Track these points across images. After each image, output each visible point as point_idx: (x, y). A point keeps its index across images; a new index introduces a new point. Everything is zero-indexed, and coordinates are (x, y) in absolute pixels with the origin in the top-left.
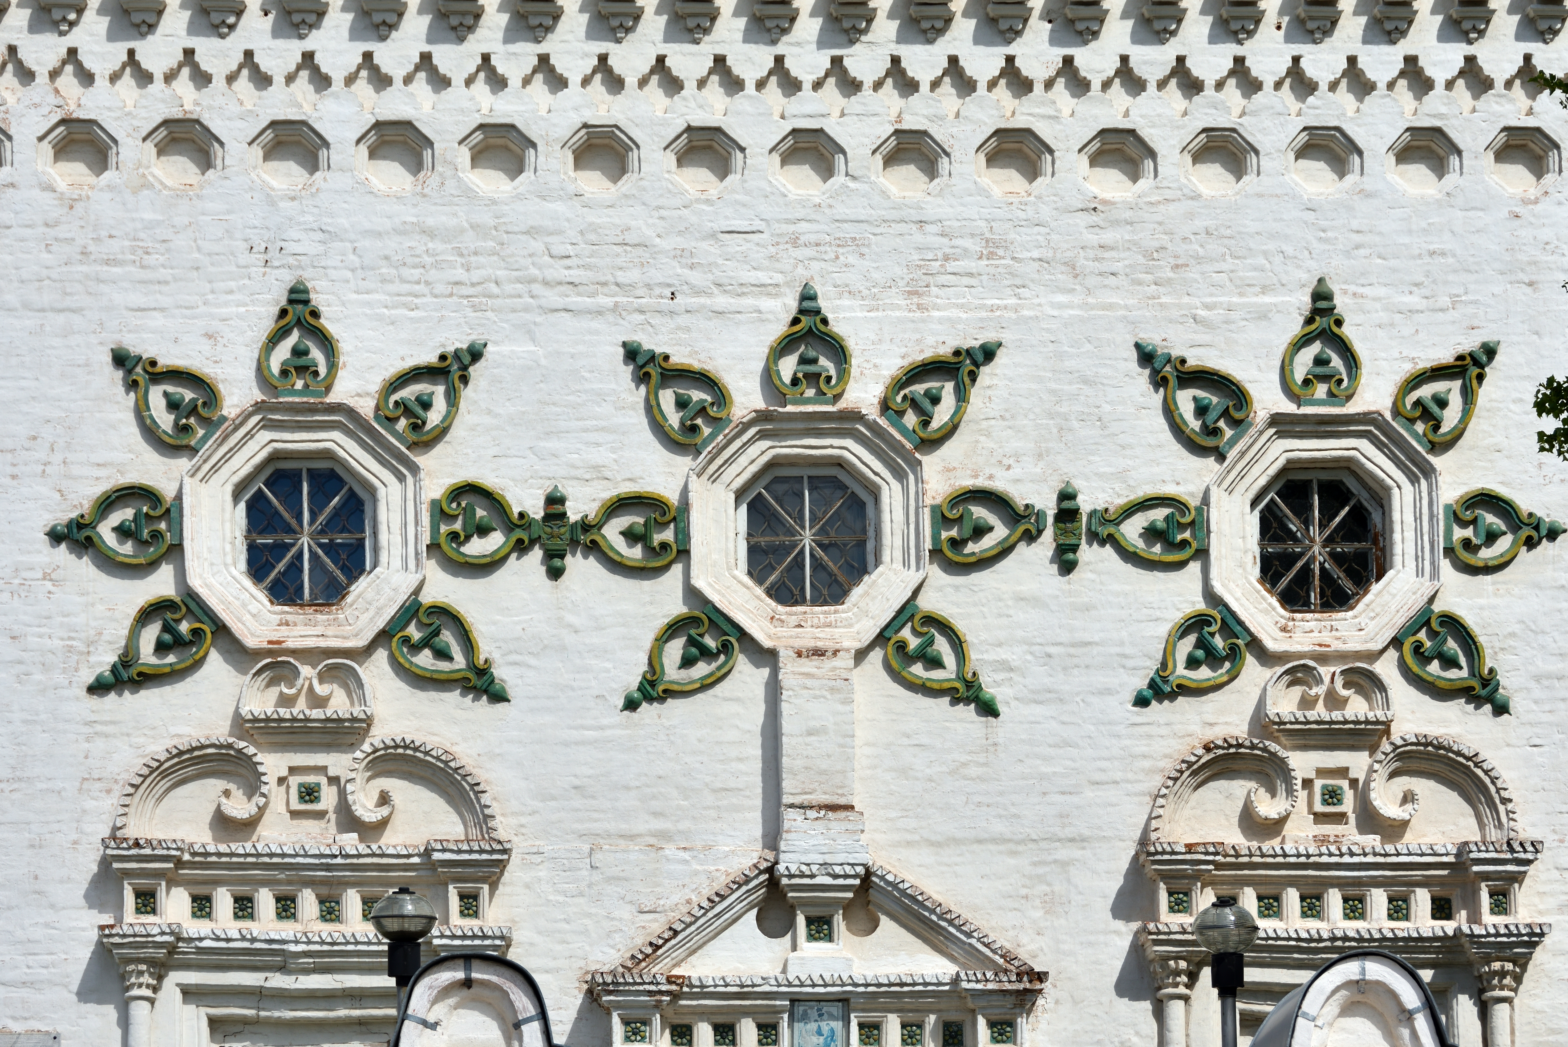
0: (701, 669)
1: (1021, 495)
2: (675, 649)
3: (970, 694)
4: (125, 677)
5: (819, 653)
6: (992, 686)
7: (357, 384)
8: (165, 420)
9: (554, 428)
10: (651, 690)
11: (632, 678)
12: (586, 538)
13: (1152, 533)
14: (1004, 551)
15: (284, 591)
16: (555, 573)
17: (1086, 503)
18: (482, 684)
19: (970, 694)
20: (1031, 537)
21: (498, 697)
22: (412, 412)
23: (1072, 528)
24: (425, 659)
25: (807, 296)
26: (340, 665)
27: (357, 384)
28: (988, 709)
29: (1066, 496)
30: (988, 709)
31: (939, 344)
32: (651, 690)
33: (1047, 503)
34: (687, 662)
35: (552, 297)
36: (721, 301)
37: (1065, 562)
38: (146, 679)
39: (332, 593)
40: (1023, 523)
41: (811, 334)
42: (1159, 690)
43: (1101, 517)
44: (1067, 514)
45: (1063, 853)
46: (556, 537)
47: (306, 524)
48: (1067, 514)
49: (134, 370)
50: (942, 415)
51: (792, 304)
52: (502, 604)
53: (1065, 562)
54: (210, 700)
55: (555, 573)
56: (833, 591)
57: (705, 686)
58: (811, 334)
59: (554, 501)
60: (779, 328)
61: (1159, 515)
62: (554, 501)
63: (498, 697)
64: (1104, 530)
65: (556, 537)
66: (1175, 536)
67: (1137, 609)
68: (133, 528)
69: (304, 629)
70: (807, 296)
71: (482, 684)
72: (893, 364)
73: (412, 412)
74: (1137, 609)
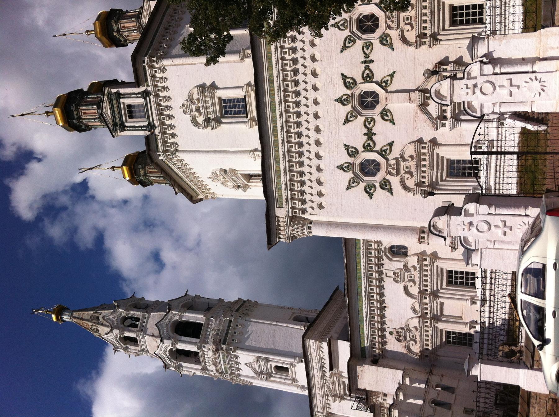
0: (388, 114)
1: (363, 69)
2: (386, 118)
3: (392, 76)
4: (390, 191)
5: (386, 98)
6: (391, 72)
7: (350, 175)
8: (355, 184)
9: (355, 134)
10: (392, 121)
11: (390, 124)
12: (369, 130)
13: (368, 49)
14: (371, 71)
15: (378, 170)
16: (375, 134)
17: (364, 60)
18: (391, 144)
19: (392, 76)
20: (368, 67)
21: (393, 142)
22: (353, 153)
23: (367, 61)
24: (388, 152)
25: (336, 100)
26: (388, 165)
27: (350, 175)
28: (394, 72)
29: (362, 62)
30: (394, 72)
31: (341, 82)
32: (392, 121)
33: (364, 65)
34: (388, 116)
35: (337, 135)
36: (337, 112)
37: (372, 61)
38: (391, 189)
39: (378, 164)
40: (367, 68)
41: (341, 101)
42: (391, 47)
43: (365, 57)
44: (364, 62)
45: (417, 60)
46: (370, 134)
47: (370, 168)
48: (364, 62)
49: (349, 187)
50: (351, 81)
51: (336, 103)
52: (380, 142)
53: (372, 61)
54: (395, 181)
55: (375, 134)
56: (377, 96)
57: (391, 114)
58: (341, 101)
59: (365, 134)
60: (340, 104)
61: (365, 48)
62: (365, 134)
63: (393, 142)
64: (367, 56)
65: (370, 134)
66: (368, 45)
67: (379, 52)
68: (369, 191)
69: (384, 167)
70: (336, 100)
71: (391, 144)
72: (345, 88)
73: (353, 153)
74: (379, 52)
